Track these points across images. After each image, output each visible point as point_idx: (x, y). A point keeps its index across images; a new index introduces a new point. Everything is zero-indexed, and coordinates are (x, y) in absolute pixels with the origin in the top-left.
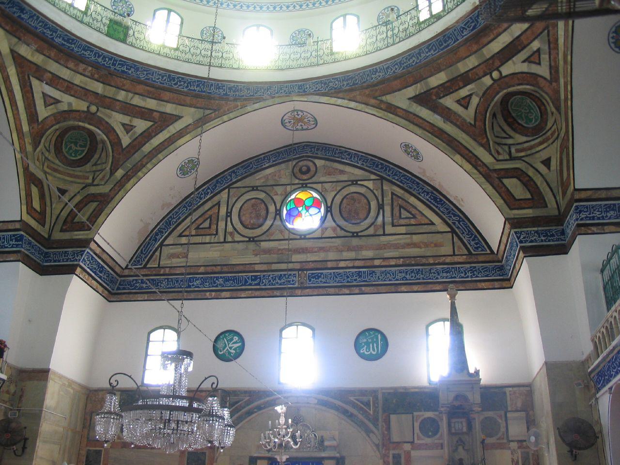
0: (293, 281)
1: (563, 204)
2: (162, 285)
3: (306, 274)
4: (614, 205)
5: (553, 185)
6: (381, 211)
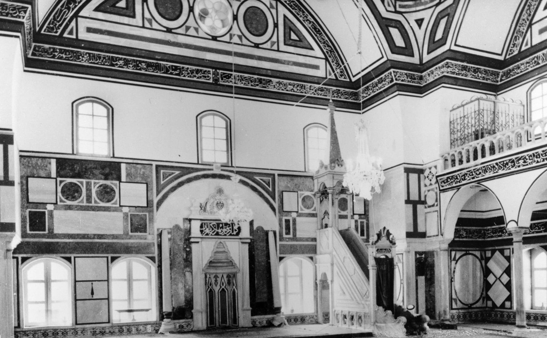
0: (208, 77)
1: (426, 58)
2: (84, 59)
3: (218, 73)
4: (467, 66)
5: (420, 41)
6: (276, 29)
